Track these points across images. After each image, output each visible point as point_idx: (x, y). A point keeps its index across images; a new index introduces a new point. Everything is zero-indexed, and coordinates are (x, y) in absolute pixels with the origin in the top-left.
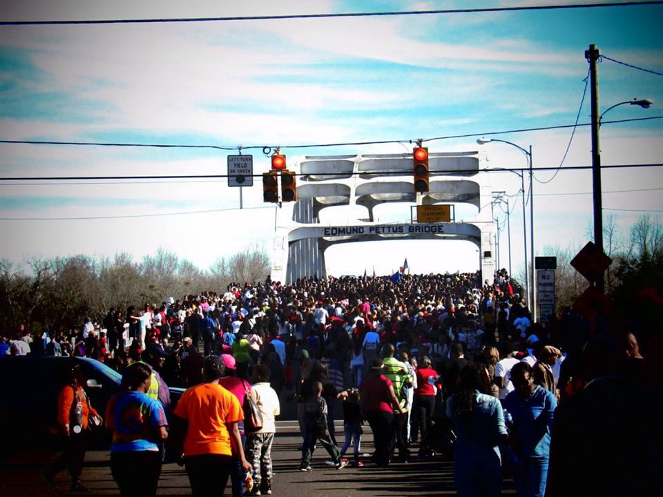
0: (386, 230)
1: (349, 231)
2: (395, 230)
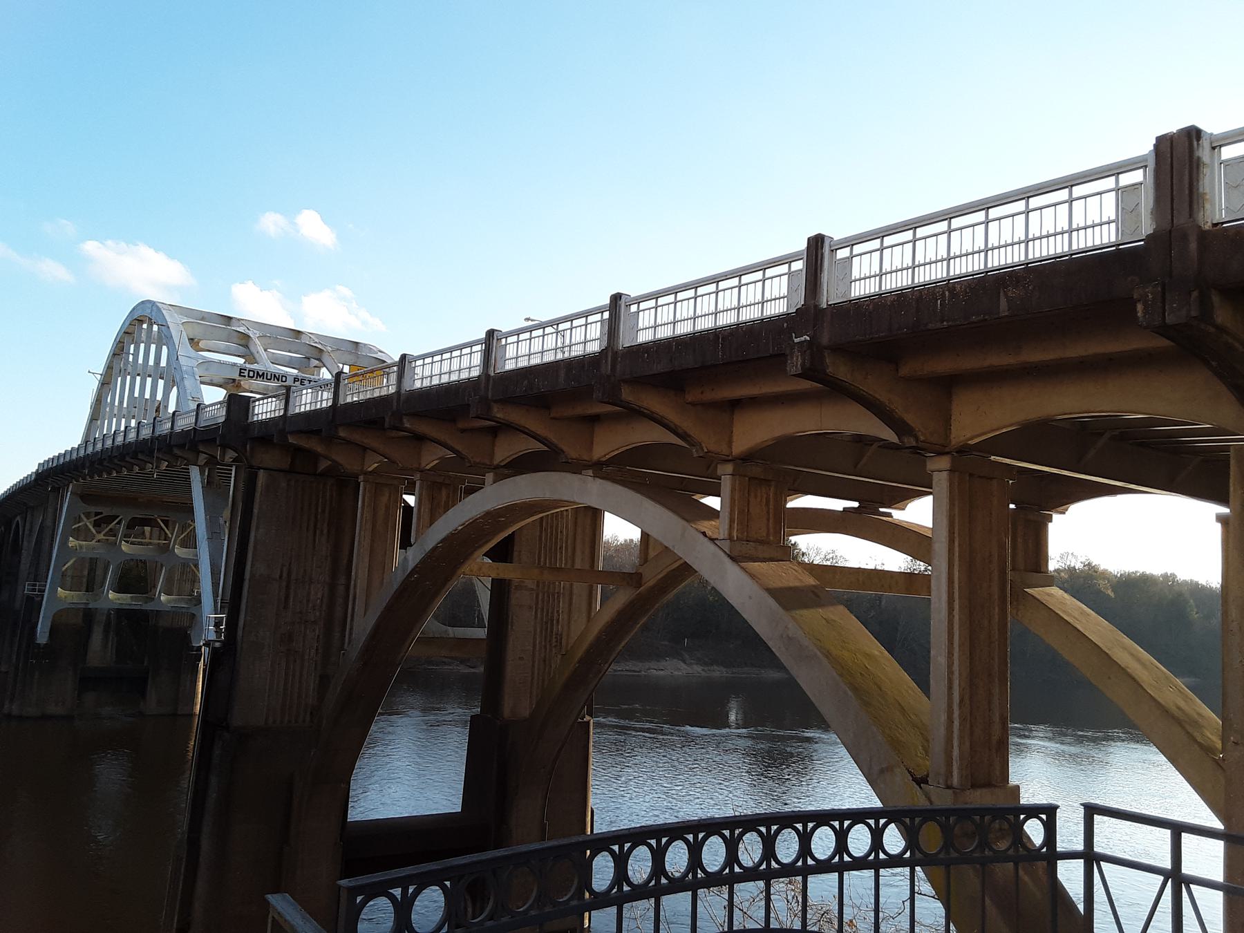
1: (269, 377)
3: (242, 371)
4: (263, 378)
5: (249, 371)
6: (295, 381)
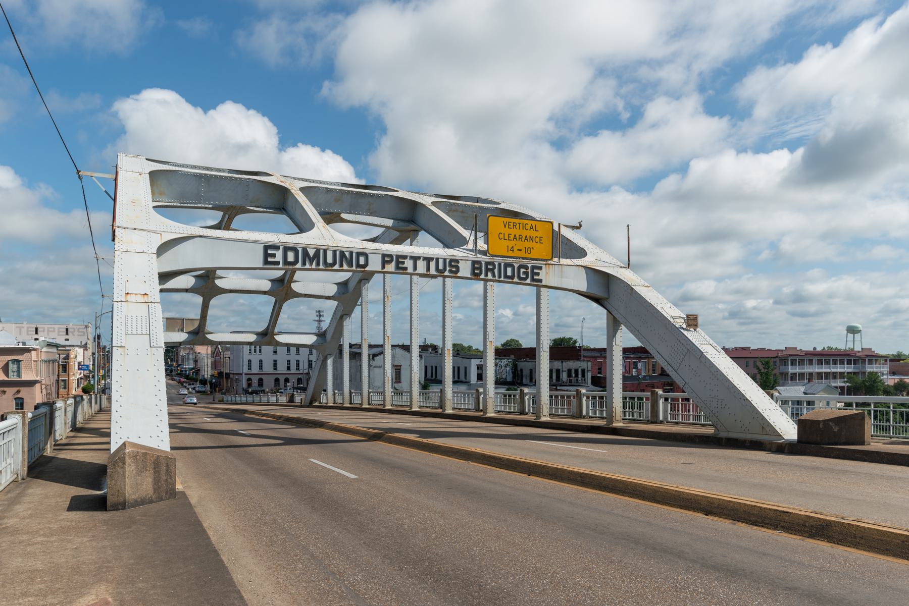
0: (421, 266)
1: (330, 260)
2: (441, 267)
4: (318, 264)
5: (286, 249)
6: (384, 263)
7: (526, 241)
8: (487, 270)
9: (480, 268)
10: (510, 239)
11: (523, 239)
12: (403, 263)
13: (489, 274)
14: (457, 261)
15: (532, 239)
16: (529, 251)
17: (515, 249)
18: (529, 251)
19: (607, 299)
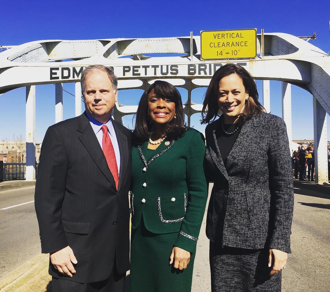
2: (165, 71)
3: (53, 71)
5: (63, 69)
6: (124, 71)
7: (233, 46)
8: (200, 70)
9: (195, 70)
10: (219, 46)
11: (230, 45)
12: (137, 71)
13: (202, 72)
14: (176, 66)
15: (238, 44)
16: (236, 54)
17: (224, 53)
18: (236, 54)
19: (310, 83)
